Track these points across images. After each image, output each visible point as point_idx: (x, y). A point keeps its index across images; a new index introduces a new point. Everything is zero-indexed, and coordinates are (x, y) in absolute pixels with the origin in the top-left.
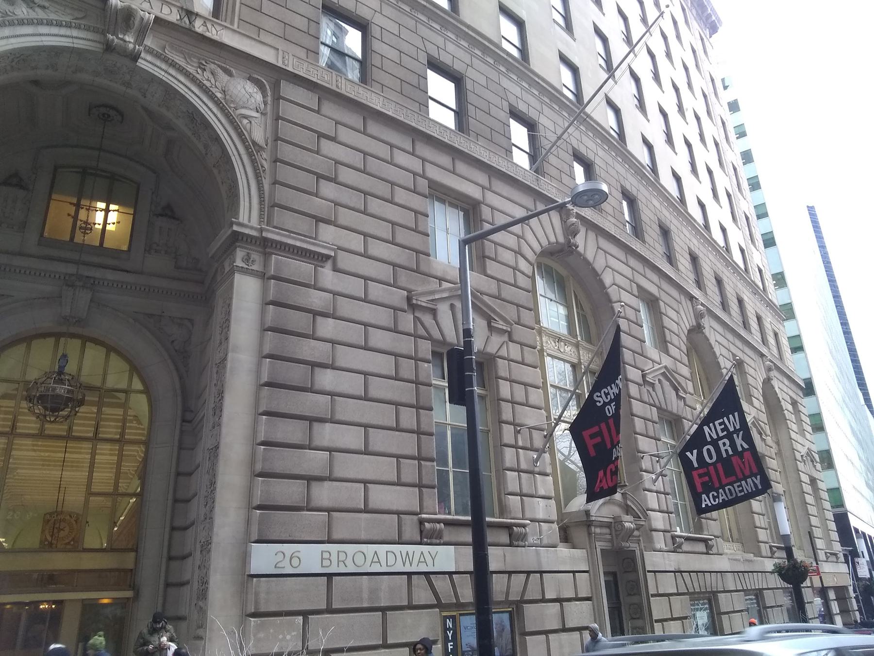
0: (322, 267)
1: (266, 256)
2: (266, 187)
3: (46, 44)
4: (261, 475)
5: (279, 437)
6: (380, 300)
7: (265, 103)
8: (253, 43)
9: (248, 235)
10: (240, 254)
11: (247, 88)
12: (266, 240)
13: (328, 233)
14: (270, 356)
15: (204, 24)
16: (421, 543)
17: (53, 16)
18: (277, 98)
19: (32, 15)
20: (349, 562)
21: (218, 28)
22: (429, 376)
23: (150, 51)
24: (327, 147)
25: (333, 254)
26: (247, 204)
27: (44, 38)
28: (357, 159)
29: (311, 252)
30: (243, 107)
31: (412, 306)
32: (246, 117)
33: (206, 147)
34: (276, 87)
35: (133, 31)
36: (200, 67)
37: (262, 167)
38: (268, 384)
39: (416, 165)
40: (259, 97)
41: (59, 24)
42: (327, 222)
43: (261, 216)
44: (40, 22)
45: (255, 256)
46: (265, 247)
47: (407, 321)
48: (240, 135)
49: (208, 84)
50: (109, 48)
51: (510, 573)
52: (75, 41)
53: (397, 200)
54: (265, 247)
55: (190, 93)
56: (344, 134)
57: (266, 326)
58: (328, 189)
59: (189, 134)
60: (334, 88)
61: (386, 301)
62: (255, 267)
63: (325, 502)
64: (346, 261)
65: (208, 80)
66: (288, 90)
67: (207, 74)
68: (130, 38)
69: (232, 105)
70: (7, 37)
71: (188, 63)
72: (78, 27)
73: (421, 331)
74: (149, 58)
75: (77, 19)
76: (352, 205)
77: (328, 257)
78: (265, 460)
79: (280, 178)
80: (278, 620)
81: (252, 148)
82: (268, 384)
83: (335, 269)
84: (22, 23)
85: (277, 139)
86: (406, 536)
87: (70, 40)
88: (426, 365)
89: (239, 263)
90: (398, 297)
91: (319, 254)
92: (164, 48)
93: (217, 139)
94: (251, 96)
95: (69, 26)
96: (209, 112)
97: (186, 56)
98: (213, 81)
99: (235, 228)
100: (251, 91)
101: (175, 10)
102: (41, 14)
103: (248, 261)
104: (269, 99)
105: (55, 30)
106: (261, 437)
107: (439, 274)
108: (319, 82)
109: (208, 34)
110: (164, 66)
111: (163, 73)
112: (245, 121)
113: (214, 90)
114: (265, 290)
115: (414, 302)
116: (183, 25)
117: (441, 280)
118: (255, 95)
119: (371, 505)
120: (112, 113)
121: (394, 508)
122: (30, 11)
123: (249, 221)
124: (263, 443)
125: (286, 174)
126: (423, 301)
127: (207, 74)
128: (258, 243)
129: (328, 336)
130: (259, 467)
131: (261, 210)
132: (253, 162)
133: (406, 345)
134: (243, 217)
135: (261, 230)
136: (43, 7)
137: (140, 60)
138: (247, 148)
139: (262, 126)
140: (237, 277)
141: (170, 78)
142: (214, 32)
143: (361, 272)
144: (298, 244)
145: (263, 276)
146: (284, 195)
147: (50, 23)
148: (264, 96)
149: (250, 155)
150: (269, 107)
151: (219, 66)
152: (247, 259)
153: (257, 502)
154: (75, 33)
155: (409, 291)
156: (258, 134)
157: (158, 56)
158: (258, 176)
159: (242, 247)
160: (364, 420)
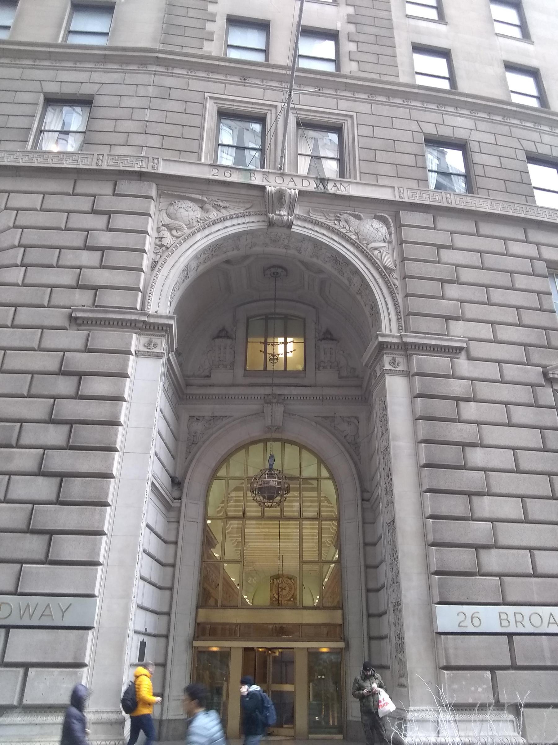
0: (457, 358)
1: (408, 357)
2: (400, 300)
3: (230, 233)
4: (433, 544)
5: (444, 510)
6: (517, 379)
7: (390, 233)
8: (374, 188)
9: (391, 343)
10: (387, 359)
11: (374, 225)
12: (406, 344)
13: (458, 329)
14: (425, 441)
15: (335, 186)
17: (233, 212)
18: (399, 226)
19: (220, 215)
20: (526, 622)
21: (345, 185)
23: (299, 218)
24: (446, 255)
25: (465, 345)
26: (387, 318)
27: (229, 229)
28: (475, 259)
29: (445, 347)
30: (373, 242)
32: (376, 249)
33: (349, 280)
34: (396, 217)
35: (285, 206)
36: (336, 220)
37: (395, 285)
38: (427, 465)
39: (531, 250)
40: (384, 230)
41: (237, 217)
42: (456, 319)
43: (399, 325)
44: (226, 219)
45: (399, 359)
46: (406, 350)
48: (374, 264)
49: (344, 231)
50: (271, 224)
52: (248, 225)
53: (517, 286)
54: (406, 350)
55: (332, 241)
56: (460, 241)
57: (417, 416)
58: (452, 291)
59: (335, 272)
60: (445, 204)
61: (522, 380)
62: (400, 368)
64: (477, 349)
65: (343, 228)
66: (407, 217)
67: (342, 223)
68: (284, 213)
69: (364, 242)
70: (207, 236)
71: (327, 219)
72: (249, 215)
74: (299, 223)
75: (247, 209)
76: (476, 299)
77: (461, 349)
78: (435, 531)
79: (410, 291)
80: (468, 673)
81: (384, 272)
82: (427, 465)
83: (469, 358)
84: (215, 223)
85: (403, 259)
87: (245, 225)
89: (387, 367)
90: (533, 374)
91: (453, 347)
92: (308, 213)
93: (357, 272)
94: (378, 231)
95: (243, 216)
96: (348, 253)
98: (347, 227)
99: (380, 339)
100: (377, 227)
101: (312, 181)
102: (225, 213)
103: (394, 363)
104: (393, 229)
105: (235, 221)
106: (429, 512)
108: (431, 203)
109: (339, 192)
110: (310, 226)
111: (310, 232)
112: (376, 252)
113: (348, 234)
114: (411, 386)
115: (551, 376)
116: (320, 190)
118: (381, 229)
120: (279, 270)
122: (218, 212)
123: (391, 331)
124: (431, 517)
125: (415, 286)
127: (342, 223)
128: (400, 348)
129: (473, 418)
130: (431, 538)
131: (398, 320)
132: (387, 283)
134: (385, 329)
135: (401, 337)
136: (225, 208)
137: (293, 227)
138: (380, 273)
139: (390, 252)
140: (388, 378)
141: (316, 234)
142: (343, 189)
143: (494, 357)
144: (433, 342)
145: (408, 374)
146: (416, 304)
147: (231, 218)
149: (384, 278)
150: (393, 235)
151: (350, 214)
152: (393, 362)
153: (434, 568)
154: (247, 219)
155: (544, 367)
156: (388, 260)
157: (305, 220)
158: (392, 294)
159: (388, 354)
160: (520, 492)
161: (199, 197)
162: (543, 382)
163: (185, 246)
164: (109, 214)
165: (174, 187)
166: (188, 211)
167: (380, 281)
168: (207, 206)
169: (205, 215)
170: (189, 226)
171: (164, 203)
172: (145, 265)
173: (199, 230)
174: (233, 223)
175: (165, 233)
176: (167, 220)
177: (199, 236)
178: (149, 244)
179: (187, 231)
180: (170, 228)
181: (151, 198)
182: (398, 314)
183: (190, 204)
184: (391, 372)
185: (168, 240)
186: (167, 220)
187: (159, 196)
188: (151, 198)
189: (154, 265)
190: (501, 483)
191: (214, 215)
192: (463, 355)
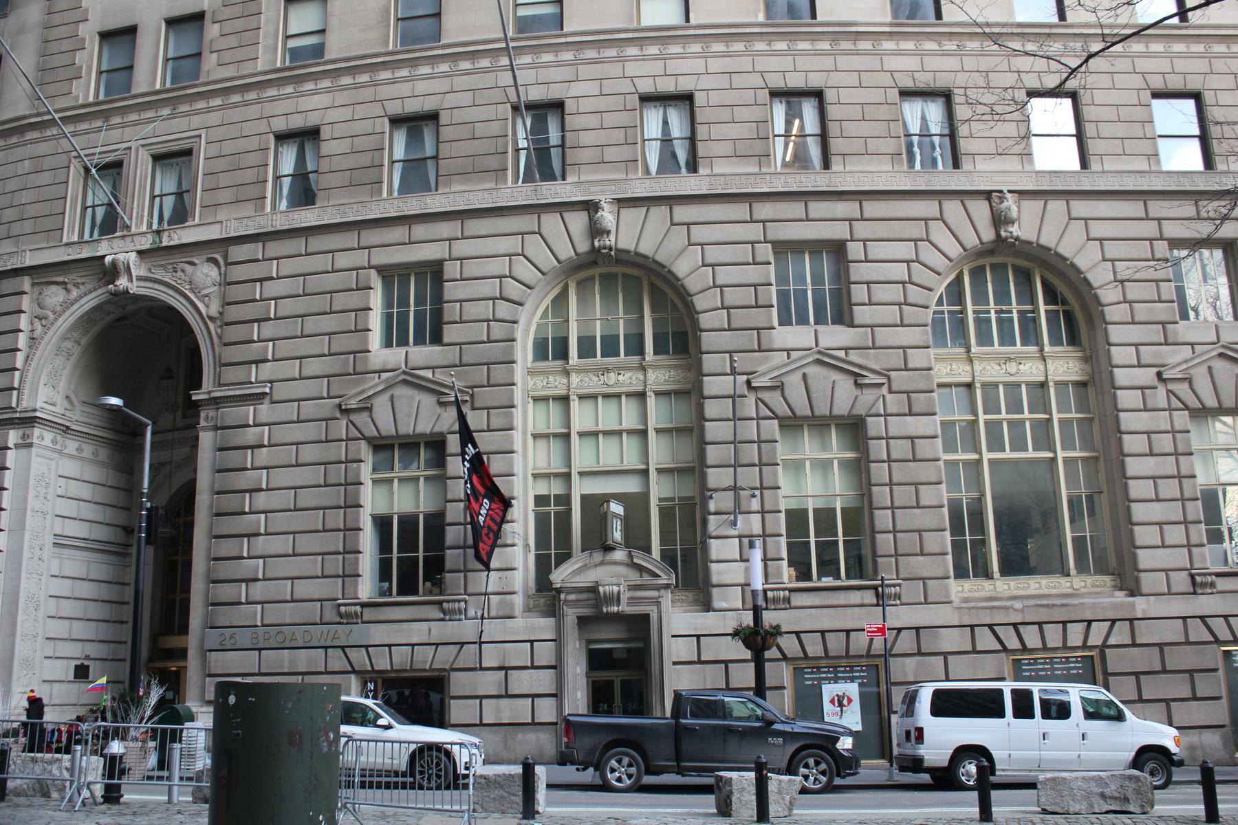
16: (339, 623)
22: (358, 474)
23: (140, 279)
28: (296, 285)
50: (116, 294)
63: (258, 598)
66: (238, 253)
67: (180, 274)
86: (327, 618)
88: (355, 465)
99: (194, 398)
107: (378, 368)
117: (379, 372)
119: (296, 597)
121: (316, 597)
125: (234, 333)
126: (353, 403)
127: (180, 274)
129: (263, 464)
133: (340, 451)
135: (209, 393)
138: (205, 323)
144: (237, 393)
148: (219, 267)
160: (291, 529)
161: (61, 279)
162: (338, 415)
166: (54, 296)
167: (205, 332)
170: (54, 312)
173: (60, 315)
176: (38, 311)
177: (61, 320)
180: (40, 319)
183: (54, 288)
184: (205, 429)
186: (38, 311)
187: (33, 285)
190: (281, 522)
192: (267, 400)
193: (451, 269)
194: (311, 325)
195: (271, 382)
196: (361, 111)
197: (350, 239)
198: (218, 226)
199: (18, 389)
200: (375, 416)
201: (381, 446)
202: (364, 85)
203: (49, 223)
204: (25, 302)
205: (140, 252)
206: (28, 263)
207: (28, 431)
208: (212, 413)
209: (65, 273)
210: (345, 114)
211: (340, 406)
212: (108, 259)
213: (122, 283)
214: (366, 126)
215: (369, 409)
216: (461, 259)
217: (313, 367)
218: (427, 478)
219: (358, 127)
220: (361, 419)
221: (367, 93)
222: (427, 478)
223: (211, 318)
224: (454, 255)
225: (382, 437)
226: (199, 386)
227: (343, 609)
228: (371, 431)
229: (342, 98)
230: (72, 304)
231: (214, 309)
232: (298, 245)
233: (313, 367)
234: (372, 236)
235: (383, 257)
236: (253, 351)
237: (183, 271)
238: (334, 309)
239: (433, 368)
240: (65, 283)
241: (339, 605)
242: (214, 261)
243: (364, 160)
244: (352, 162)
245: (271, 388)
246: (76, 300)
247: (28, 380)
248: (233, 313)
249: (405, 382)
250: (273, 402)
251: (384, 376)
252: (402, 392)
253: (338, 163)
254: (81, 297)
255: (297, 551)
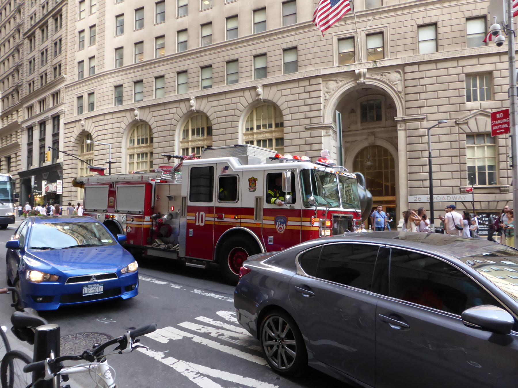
1: (405, 124)
2: (403, 103)
10: (399, 125)
22: (464, 145)
23: (368, 78)
28: (433, 80)
31: (457, 124)
47: (456, 129)
48: (394, 90)
50: (358, 84)
51: (498, 201)
64: (430, 117)
73: (462, 131)
77: (424, 118)
81: (398, 93)
89: (399, 128)
95: (349, 82)
97: (377, 74)
99: (396, 119)
102: (344, 82)
107: (469, 109)
125: (410, 97)
126: (461, 121)
131: (403, 111)
132: (399, 97)
133: (456, 138)
135: (402, 118)
138: (397, 94)
140: (399, 132)
145: (405, 130)
146: (410, 104)
149: (398, 96)
152: (401, 126)
154: (351, 83)
156: (400, 88)
157: (370, 79)
158: (401, 101)
161: (335, 79)
162: (455, 125)
163: (333, 98)
164: (310, 92)
165: (327, 77)
166: (332, 85)
167: (397, 97)
168: (338, 81)
169: (338, 85)
170: (333, 90)
171: (325, 83)
172: (322, 108)
174: (347, 85)
175: (326, 94)
176: (326, 90)
177: (336, 93)
178: (322, 100)
179: (333, 92)
180: (327, 93)
181: (320, 84)
182: (403, 109)
185: (328, 97)
187: (323, 81)
188: (320, 84)
189: (325, 106)
191: (340, 84)
192: (425, 120)
193: (496, 74)
194: (441, 94)
195: (427, 114)
196: (454, 16)
197: (455, 64)
198: (400, 59)
199: (323, 117)
200: (469, 125)
201: (471, 136)
202: (455, 6)
203: (327, 59)
204: (321, 87)
205: (368, 69)
206: (322, 73)
207: (328, 131)
208: (403, 125)
209: (335, 77)
210: (448, 17)
211: (456, 122)
212: (357, 72)
213: (362, 80)
214: (457, 22)
215: (467, 123)
216: (500, 70)
217: (442, 109)
218: (488, 146)
219: (454, 22)
220: (464, 127)
221: (456, 9)
222: (488, 146)
223: (399, 92)
224: (498, 68)
225: (472, 133)
226: (396, 116)
227: (462, 189)
228: (468, 131)
229: (445, 11)
230: (340, 87)
231: (400, 88)
232: (433, 66)
233: (442, 109)
234: (462, 63)
235: (468, 70)
236: (419, 103)
237: (385, 75)
238: (450, 88)
239: (491, 109)
240: (336, 80)
241: (460, 188)
242: (399, 72)
243: (457, 34)
244: (452, 35)
245: (427, 116)
246: (342, 86)
247: (326, 114)
248: (409, 90)
249: (481, 114)
250: (428, 121)
251: (472, 112)
252: (479, 117)
253: (446, 36)
254: (344, 85)
255: (442, 170)
